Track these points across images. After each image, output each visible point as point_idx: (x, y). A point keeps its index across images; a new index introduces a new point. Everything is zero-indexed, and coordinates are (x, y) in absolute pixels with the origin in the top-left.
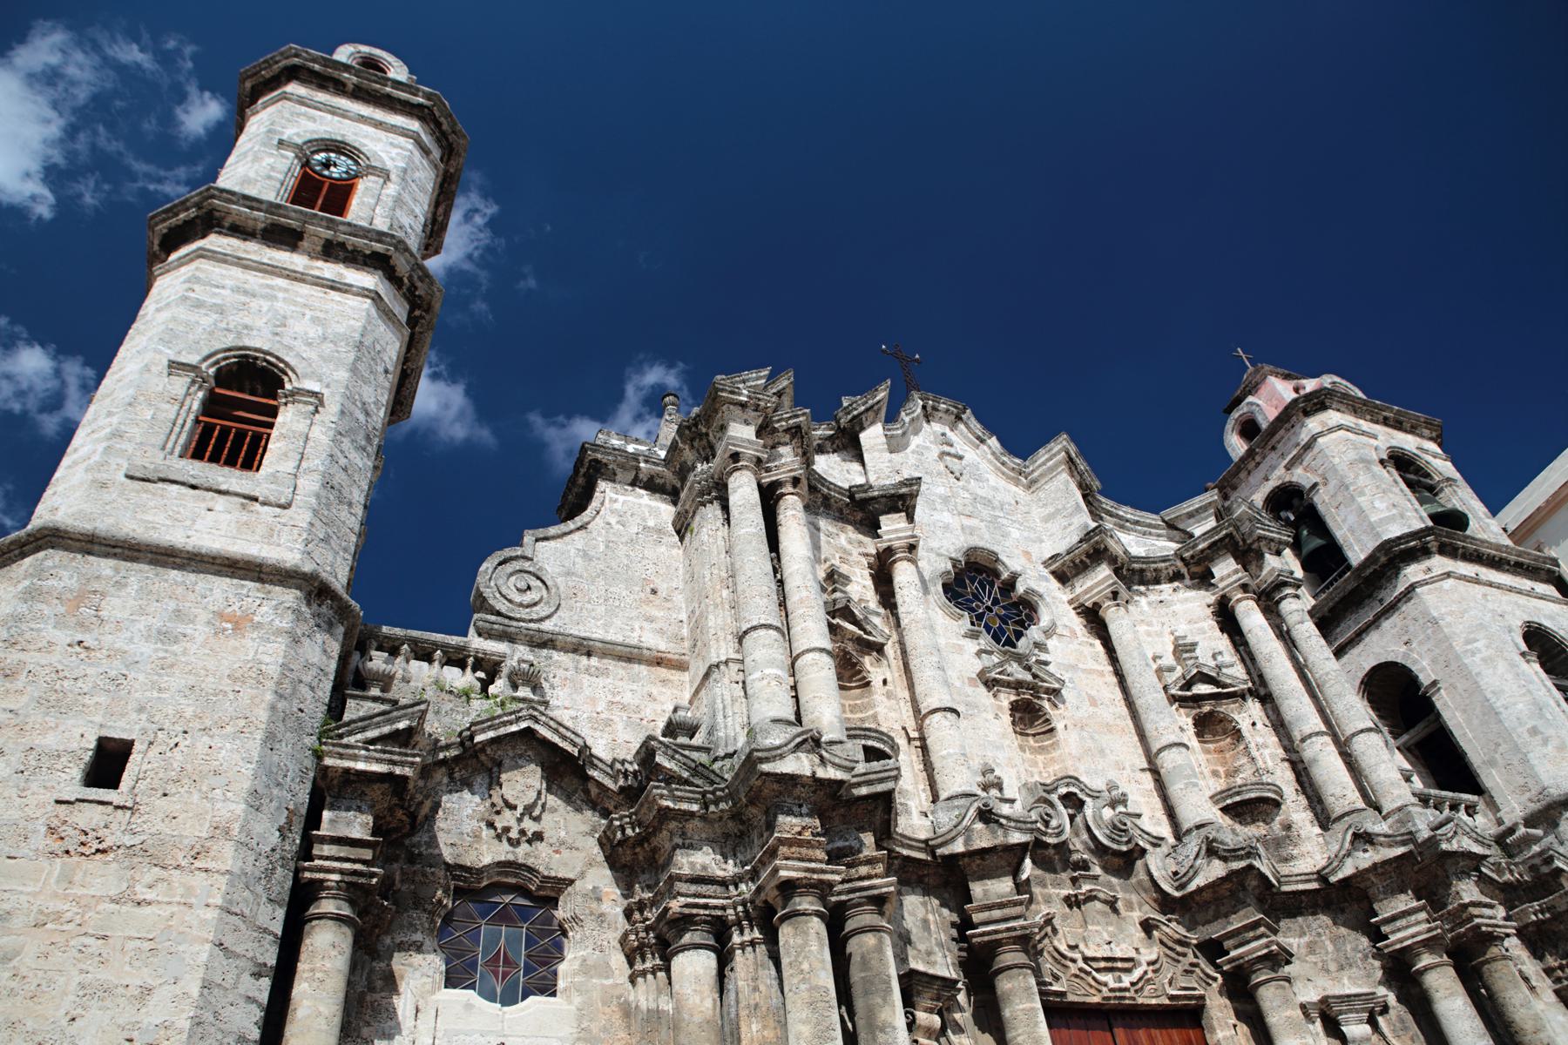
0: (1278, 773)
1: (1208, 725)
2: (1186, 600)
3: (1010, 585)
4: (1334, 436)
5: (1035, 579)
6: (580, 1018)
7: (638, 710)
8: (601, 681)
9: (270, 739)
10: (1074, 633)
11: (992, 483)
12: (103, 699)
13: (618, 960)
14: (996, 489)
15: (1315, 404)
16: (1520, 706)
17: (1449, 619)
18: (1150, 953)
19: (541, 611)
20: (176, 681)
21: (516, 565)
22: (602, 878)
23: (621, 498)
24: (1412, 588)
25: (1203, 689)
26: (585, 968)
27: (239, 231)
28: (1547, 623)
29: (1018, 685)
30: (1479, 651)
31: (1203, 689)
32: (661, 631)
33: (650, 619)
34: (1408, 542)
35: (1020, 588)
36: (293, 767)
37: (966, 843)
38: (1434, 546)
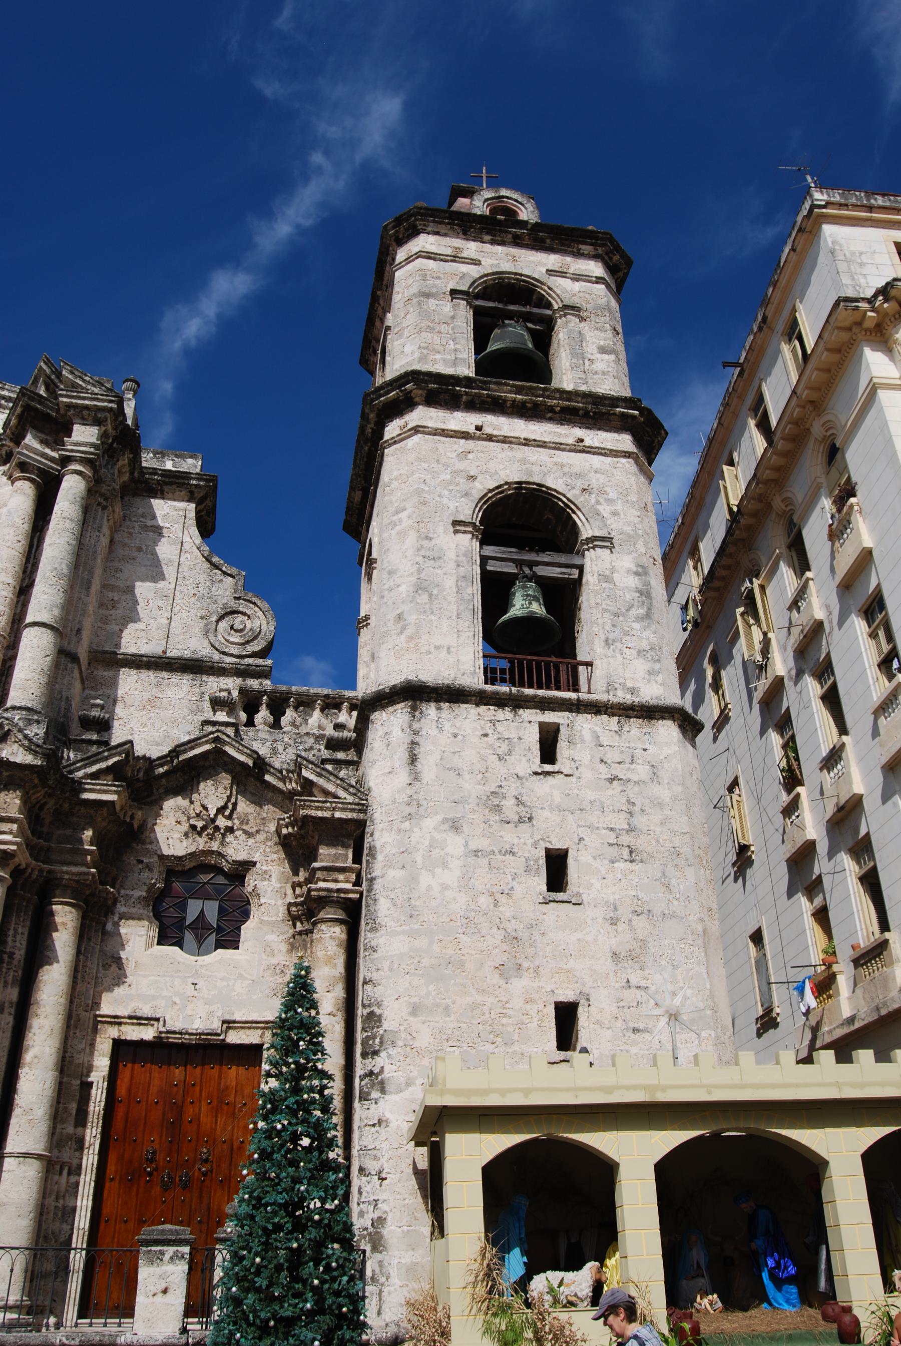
15: (406, 229)
16: (403, 588)
17: (395, 484)
30: (400, 521)
34: (388, 393)
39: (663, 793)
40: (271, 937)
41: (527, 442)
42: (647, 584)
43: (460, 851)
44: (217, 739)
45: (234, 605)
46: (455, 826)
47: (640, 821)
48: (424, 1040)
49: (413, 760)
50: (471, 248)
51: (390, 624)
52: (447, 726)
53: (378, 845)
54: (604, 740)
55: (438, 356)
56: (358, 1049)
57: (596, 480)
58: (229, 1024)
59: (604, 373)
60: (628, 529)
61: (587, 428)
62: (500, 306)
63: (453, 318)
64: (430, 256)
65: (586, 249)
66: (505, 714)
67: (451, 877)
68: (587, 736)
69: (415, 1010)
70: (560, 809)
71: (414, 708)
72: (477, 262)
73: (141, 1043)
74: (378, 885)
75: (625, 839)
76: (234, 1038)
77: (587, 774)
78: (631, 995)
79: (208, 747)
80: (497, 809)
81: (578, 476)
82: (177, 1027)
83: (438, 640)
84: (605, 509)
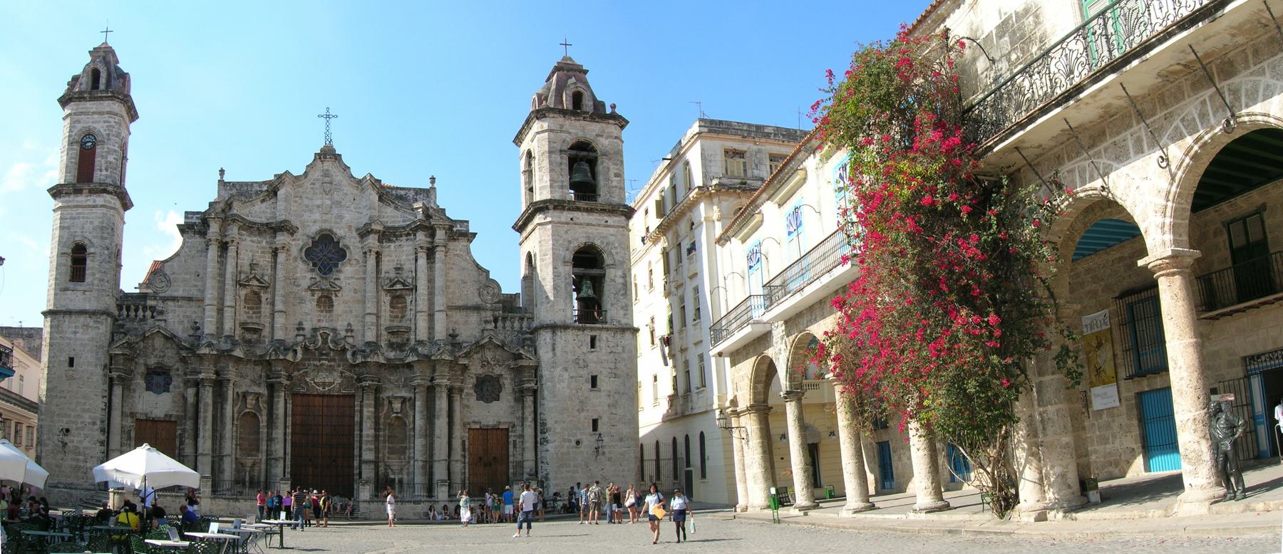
0: (413, 320)
1: (397, 299)
2: (410, 245)
3: (338, 242)
4: (543, 135)
7: (191, 317)
9: (97, 353)
10: (358, 261)
12: (67, 348)
13: (182, 385)
14: (346, 194)
17: (543, 243)
18: (339, 380)
19: (165, 289)
20: (78, 342)
22: (178, 365)
25: (398, 287)
26: (175, 387)
28: (597, 243)
31: (398, 287)
33: (196, 286)
39: (625, 356)
40: (509, 397)
41: (588, 225)
43: (567, 377)
46: (566, 369)
47: (618, 365)
48: (558, 430)
49: (554, 350)
51: (544, 300)
52: (563, 338)
53: (544, 374)
54: (609, 340)
55: (556, 184)
56: (539, 432)
57: (612, 239)
58: (500, 423)
59: (616, 187)
60: (621, 259)
62: (578, 152)
63: (561, 164)
66: (581, 332)
67: (565, 385)
68: (604, 338)
69: (556, 422)
70: (596, 363)
71: (554, 332)
72: (569, 133)
74: (544, 386)
76: (501, 427)
77: (604, 351)
79: (487, 340)
80: (578, 363)
81: (605, 237)
83: (560, 307)
84: (614, 251)
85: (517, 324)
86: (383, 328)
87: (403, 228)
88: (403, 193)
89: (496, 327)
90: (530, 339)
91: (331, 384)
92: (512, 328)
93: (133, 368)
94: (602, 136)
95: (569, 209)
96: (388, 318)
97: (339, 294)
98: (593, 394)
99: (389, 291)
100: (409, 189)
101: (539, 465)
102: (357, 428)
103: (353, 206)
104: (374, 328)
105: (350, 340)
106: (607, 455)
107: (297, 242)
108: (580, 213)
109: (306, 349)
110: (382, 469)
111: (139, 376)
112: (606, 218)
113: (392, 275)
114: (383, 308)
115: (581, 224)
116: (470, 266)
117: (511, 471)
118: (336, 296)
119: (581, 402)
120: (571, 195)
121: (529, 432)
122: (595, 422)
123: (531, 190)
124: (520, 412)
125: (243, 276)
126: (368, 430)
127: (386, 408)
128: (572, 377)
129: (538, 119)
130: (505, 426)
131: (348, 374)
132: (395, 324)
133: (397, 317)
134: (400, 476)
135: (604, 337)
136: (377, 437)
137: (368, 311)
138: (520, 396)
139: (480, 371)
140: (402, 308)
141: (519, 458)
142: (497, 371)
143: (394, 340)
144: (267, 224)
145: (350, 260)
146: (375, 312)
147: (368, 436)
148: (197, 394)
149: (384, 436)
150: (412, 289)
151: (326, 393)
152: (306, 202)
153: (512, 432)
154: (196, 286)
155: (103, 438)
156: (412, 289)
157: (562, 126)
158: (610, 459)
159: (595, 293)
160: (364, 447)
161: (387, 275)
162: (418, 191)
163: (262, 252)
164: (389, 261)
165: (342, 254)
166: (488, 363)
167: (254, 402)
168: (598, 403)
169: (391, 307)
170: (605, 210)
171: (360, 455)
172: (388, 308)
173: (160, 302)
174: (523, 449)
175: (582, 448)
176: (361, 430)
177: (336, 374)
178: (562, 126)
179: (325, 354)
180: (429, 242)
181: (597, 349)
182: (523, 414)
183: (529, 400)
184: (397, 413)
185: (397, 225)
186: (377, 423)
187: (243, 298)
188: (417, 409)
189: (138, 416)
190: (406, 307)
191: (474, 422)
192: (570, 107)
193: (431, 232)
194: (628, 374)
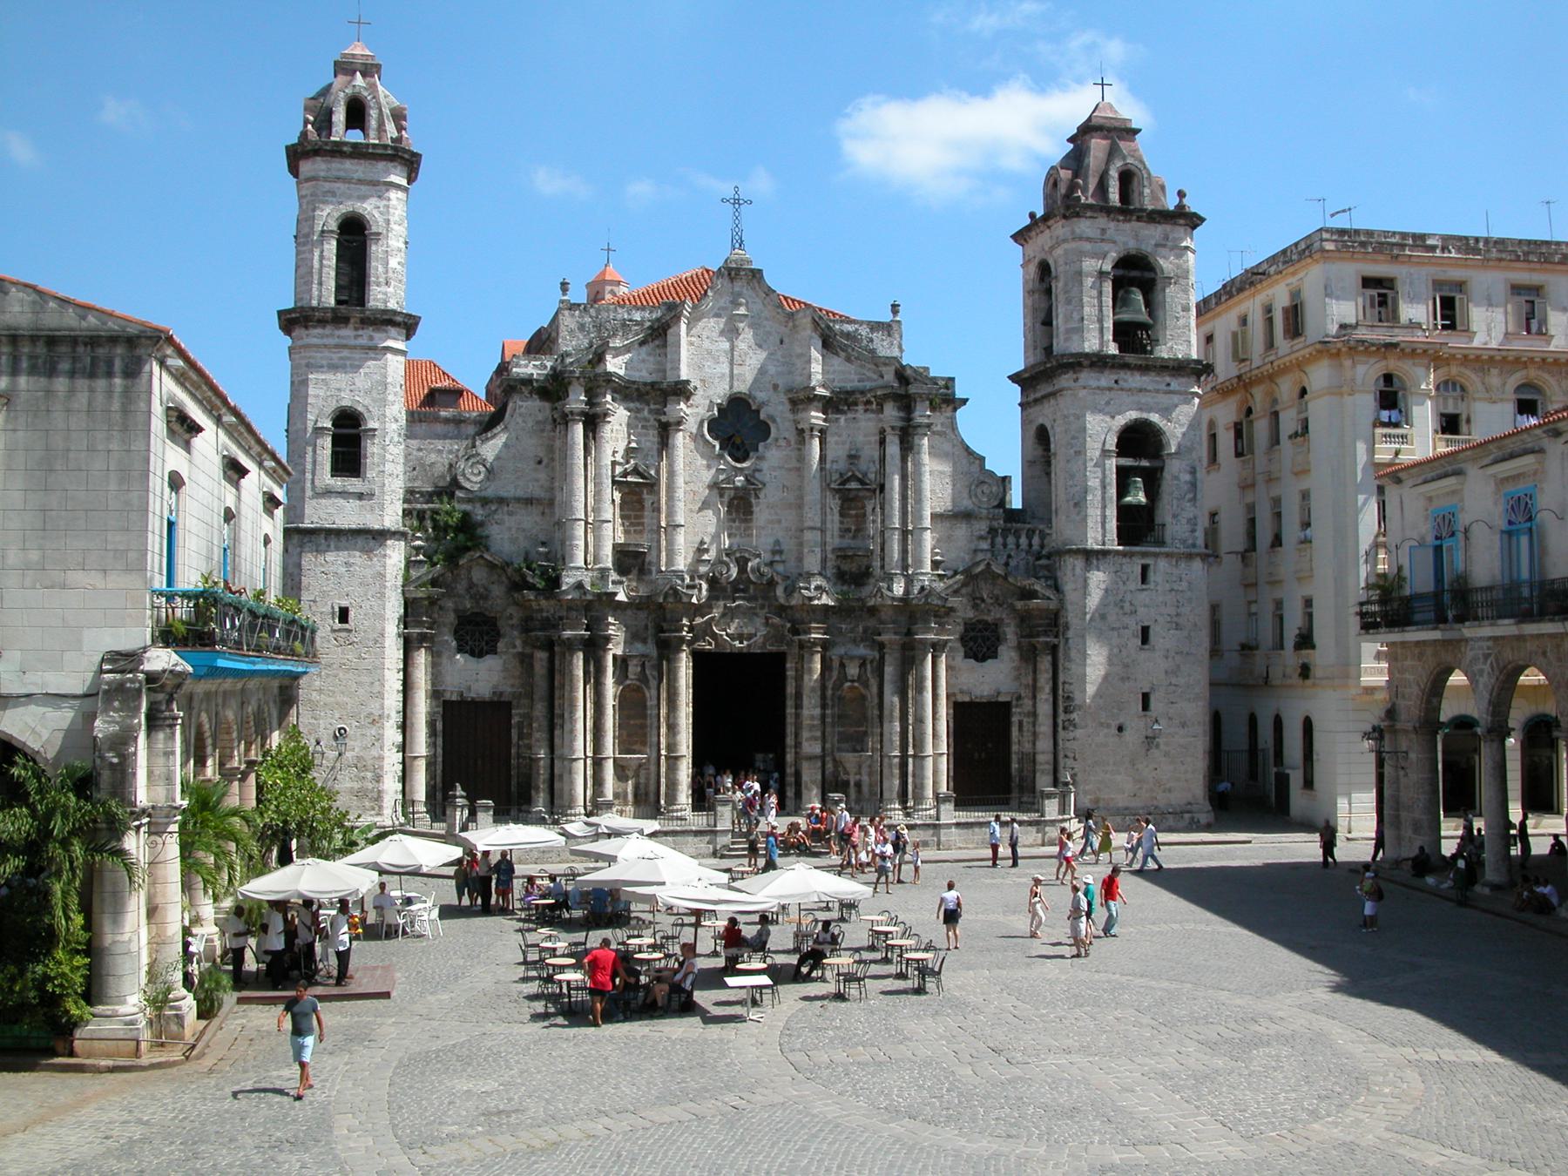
2: (869, 419)
3: (758, 412)
5: (775, 409)
6: (505, 663)
8: (513, 518)
11: (768, 329)
13: (518, 643)
14: (769, 333)
17: (1072, 418)
21: (473, 460)
23: (524, 404)
24: (1061, 390)
25: (853, 485)
27: (322, 322)
29: (736, 488)
31: (853, 485)
32: (542, 487)
33: (537, 480)
35: (762, 416)
36: (397, 604)
37: (665, 598)
38: (1086, 363)
42: (1195, 478)
44: (988, 564)
45: (982, 478)
47: (1182, 610)
50: (1112, 226)
56: (1061, 709)
61: (1173, 376)
64: (1089, 239)
65: (1182, 222)
72: (1114, 242)
73: (963, 704)
75: (1175, 619)
76: (1001, 699)
78: (1173, 688)
79: (981, 567)
80: (1122, 607)
82: (978, 693)
85: (1023, 541)
86: (829, 548)
87: (863, 393)
88: (849, 328)
89: (993, 544)
90: (1047, 567)
91: (750, 637)
92: (1018, 546)
93: (436, 616)
94: (1164, 246)
95: (1113, 367)
96: (836, 533)
97: (761, 495)
98: (1143, 655)
99: (837, 491)
100: (861, 323)
101: (1061, 755)
102: (790, 703)
103: (779, 353)
104: (818, 550)
105: (780, 568)
106: (1162, 747)
107: (696, 410)
108: (1129, 373)
109: (713, 582)
110: (830, 766)
111: (446, 630)
112: (1168, 379)
113: (842, 465)
114: (829, 517)
115: (1130, 390)
116: (959, 451)
117: (1015, 766)
118: (757, 497)
119: (1126, 666)
120: (1113, 349)
121: (1044, 708)
122: (1146, 698)
123: (1048, 322)
124: (1030, 679)
125: (619, 469)
126: (811, 709)
127: (835, 674)
128: (1113, 629)
129: (1065, 217)
130: (1008, 699)
131: (776, 620)
132: (847, 542)
133: (849, 530)
134: (858, 777)
135: (1161, 568)
136: (823, 717)
137: (809, 523)
138: (1029, 655)
139: (971, 614)
140: (857, 516)
141: (1027, 747)
142: (995, 614)
143: (845, 567)
144: (653, 384)
145: (777, 440)
146: (819, 525)
147: (812, 718)
148: (551, 661)
149: (833, 716)
150: (874, 491)
151: (745, 651)
152: (706, 344)
153: (1017, 706)
154: (537, 480)
155: (400, 739)
156: (874, 491)
157: (1103, 231)
158: (1166, 754)
159: (1147, 495)
160: (805, 734)
161: (835, 466)
162: (876, 326)
163: (643, 427)
164: (837, 443)
165: (763, 430)
166: (983, 600)
167: (639, 669)
168: (1152, 667)
169: (842, 515)
170: (1167, 367)
171: (798, 745)
172: (837, 517)
173: (478, 505)
174: (1035, 734)
175: (1127, 733)
176: (798, 706)
177: (759, 622)
178: (1103, 231)
179: (742, 591)
180: (902, 419)
181: (1152, 586)
182: (1035, 680)
183: (1045, 663)
184: (853, 681)
185: (849, 386)
186: (823, 697)
187: (618, 501)
188: (887, 677)
189: (448, 696)
190: (865, 515)
191: (962, 692)
192: (1114, 196)
193: (906, 403)
194: (1196, 625)
